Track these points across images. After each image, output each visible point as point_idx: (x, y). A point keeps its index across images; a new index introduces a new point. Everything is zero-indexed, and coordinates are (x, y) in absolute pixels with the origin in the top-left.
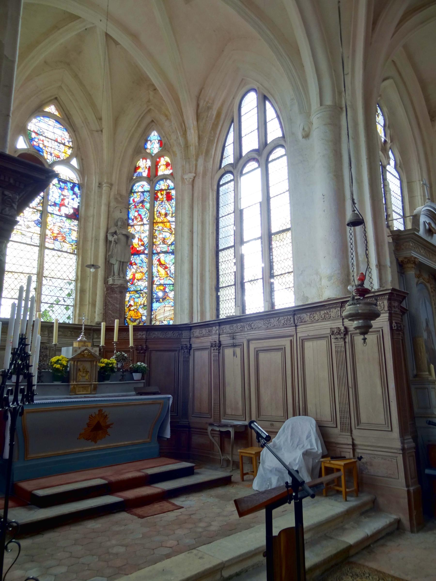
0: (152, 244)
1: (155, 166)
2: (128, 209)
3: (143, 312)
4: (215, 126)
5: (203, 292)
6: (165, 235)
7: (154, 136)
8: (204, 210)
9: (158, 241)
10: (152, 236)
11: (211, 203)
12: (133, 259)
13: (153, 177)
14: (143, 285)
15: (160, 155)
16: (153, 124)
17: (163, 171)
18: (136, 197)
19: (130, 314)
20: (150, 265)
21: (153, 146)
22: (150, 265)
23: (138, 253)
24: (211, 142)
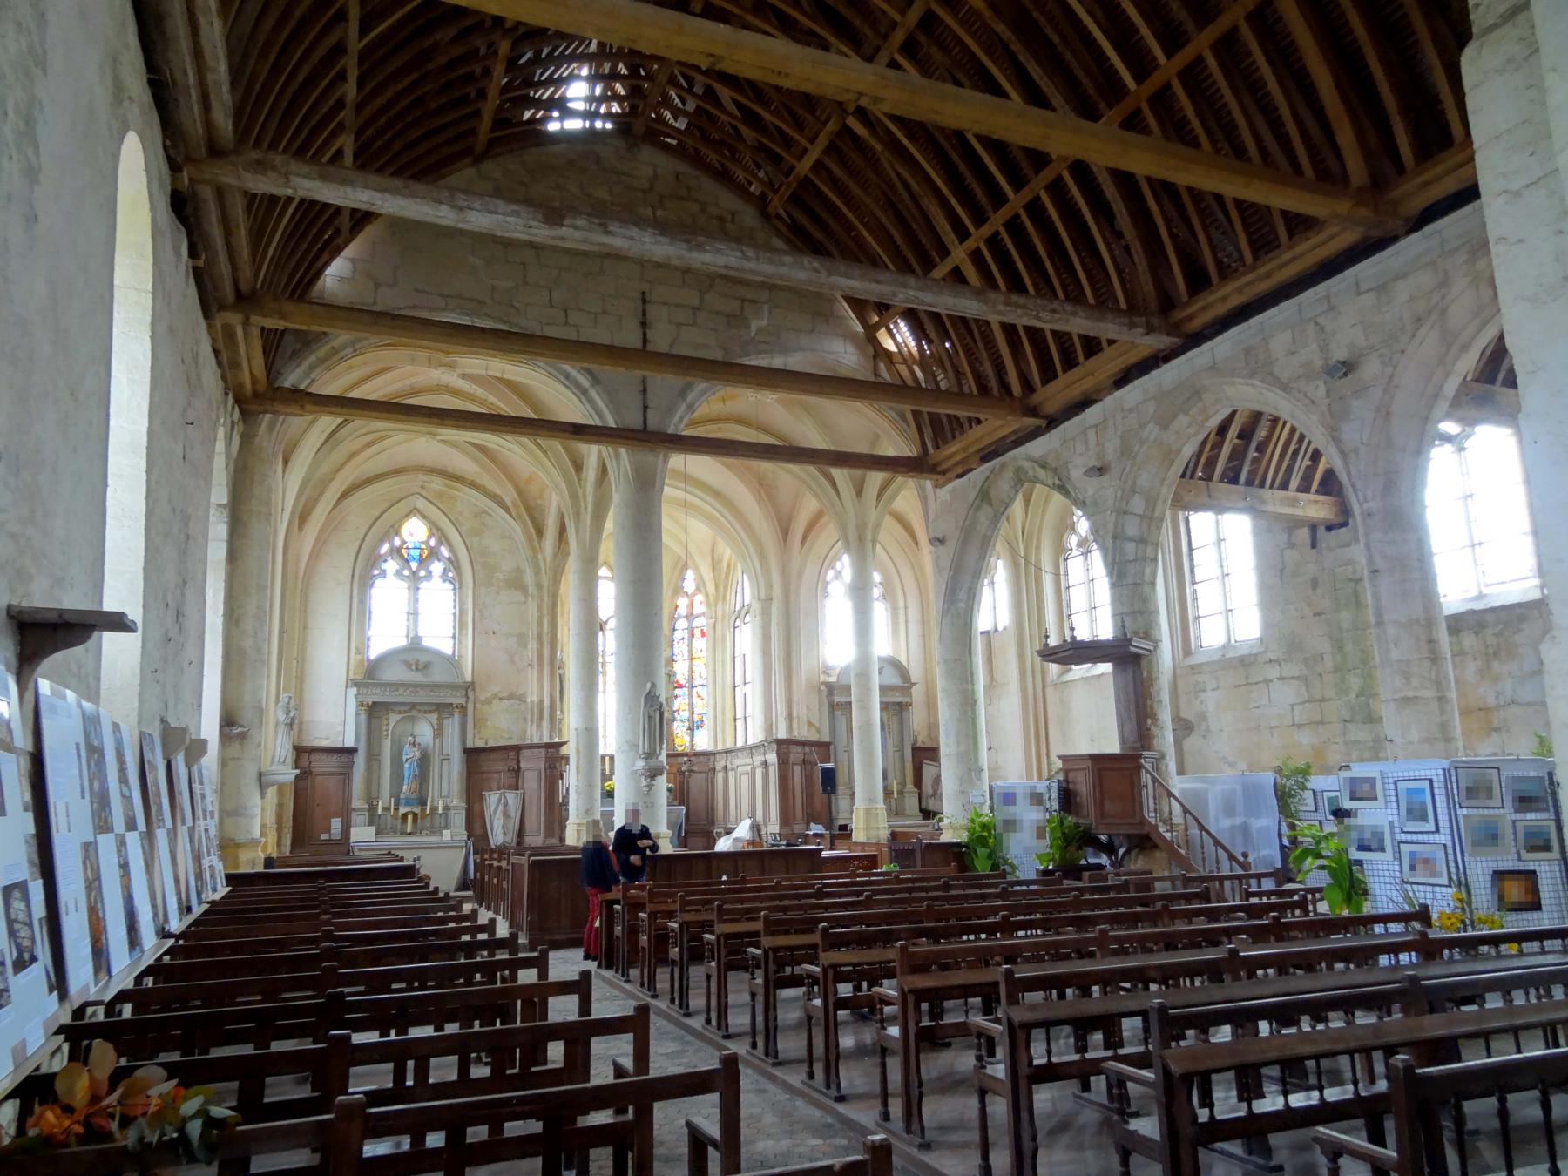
0: (691, 678)
1: (691, 605)
2: (672, 646)
3: (687, 739)
4: (727, 574)
5: (724, 722)
6: (700, 668)
7: (690, 575)
8: (724, 651)
9: (696, 675)
10: (691, 671)
11: (729, 644)
12: (677, 691)
13: (690, 617)
14: (686, 715)
15: (694, 595)
16: (685, 566)
17: (699, 608)
18: (678, 635)
19: (678, 741)
20: (690, 696)
21: (689, 584)
22: (690, 696)
23: (680, 686)
24: (725, 588)
